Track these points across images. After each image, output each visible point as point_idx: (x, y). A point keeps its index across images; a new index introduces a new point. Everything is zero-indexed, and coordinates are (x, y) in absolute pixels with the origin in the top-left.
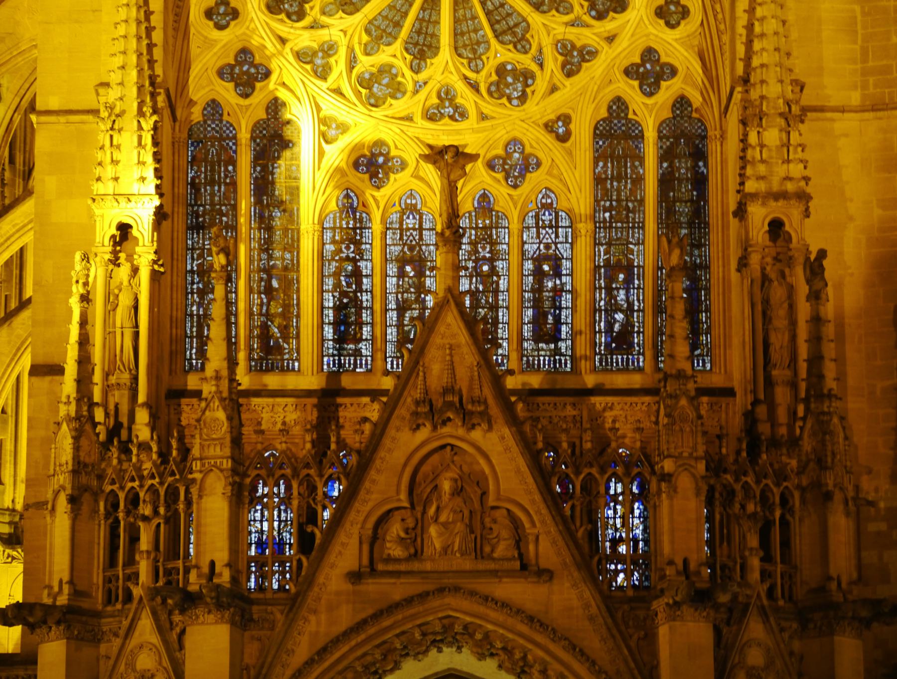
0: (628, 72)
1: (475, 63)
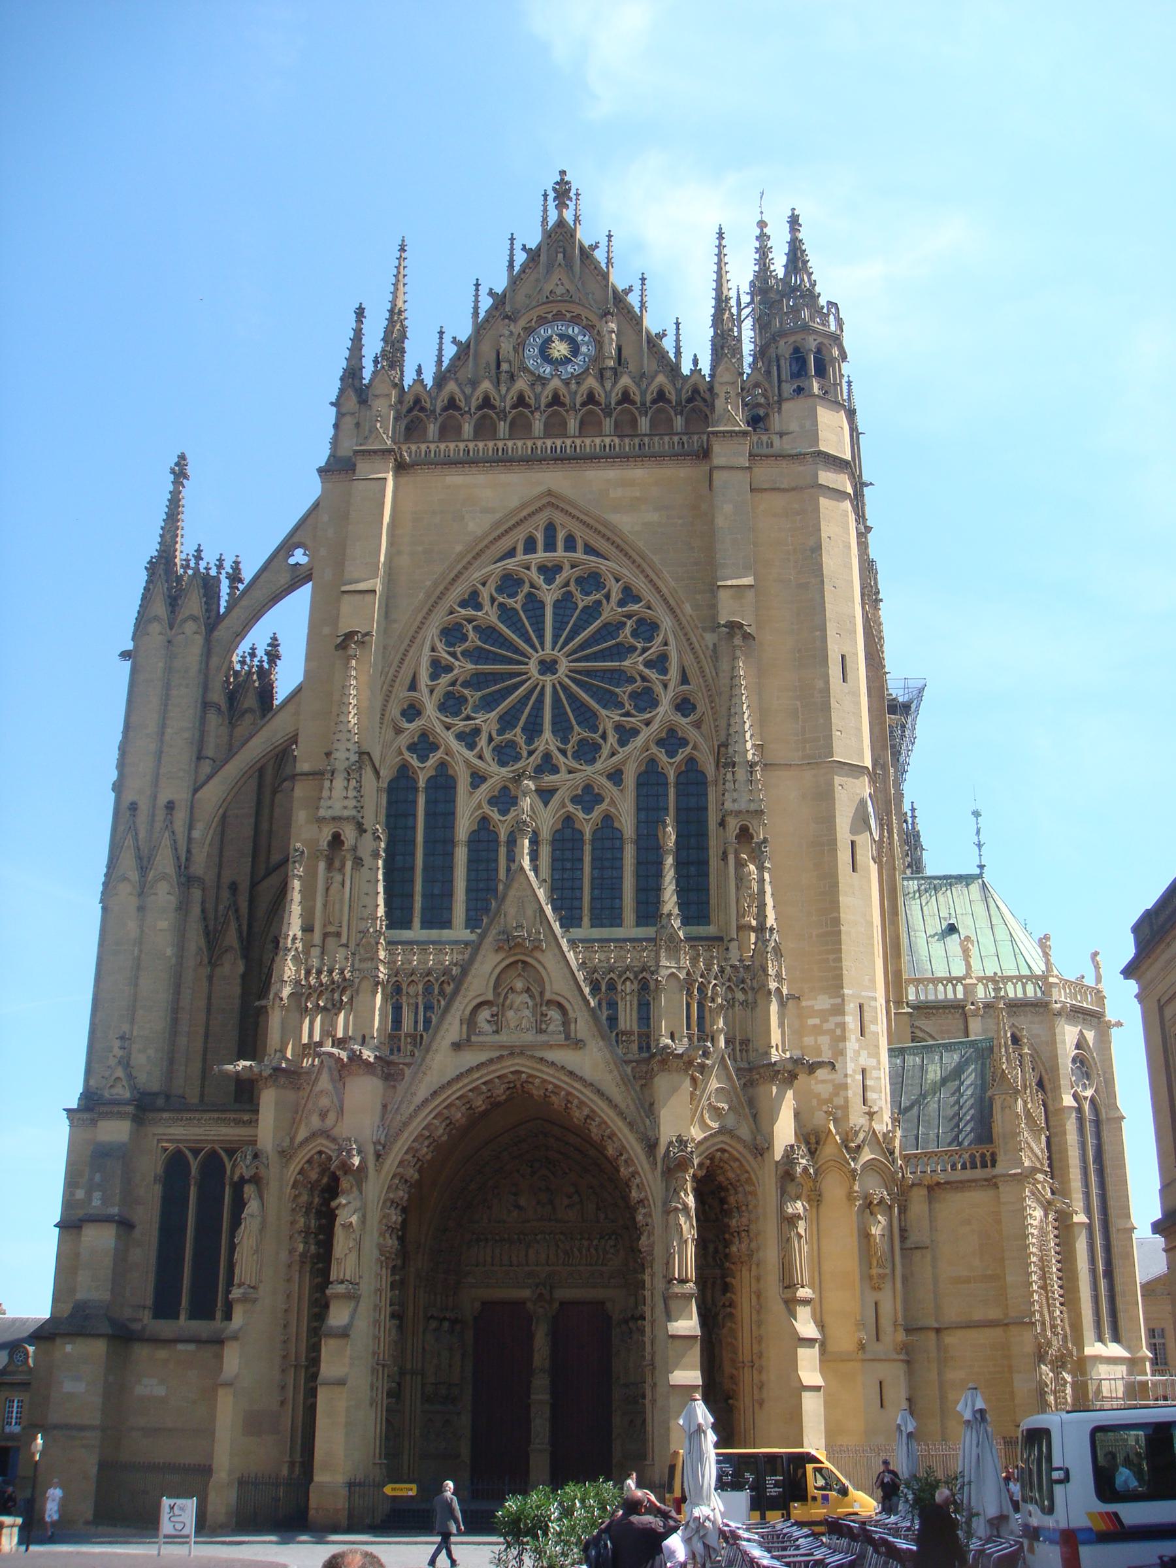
0: (660, 743)
1: (565, 741)
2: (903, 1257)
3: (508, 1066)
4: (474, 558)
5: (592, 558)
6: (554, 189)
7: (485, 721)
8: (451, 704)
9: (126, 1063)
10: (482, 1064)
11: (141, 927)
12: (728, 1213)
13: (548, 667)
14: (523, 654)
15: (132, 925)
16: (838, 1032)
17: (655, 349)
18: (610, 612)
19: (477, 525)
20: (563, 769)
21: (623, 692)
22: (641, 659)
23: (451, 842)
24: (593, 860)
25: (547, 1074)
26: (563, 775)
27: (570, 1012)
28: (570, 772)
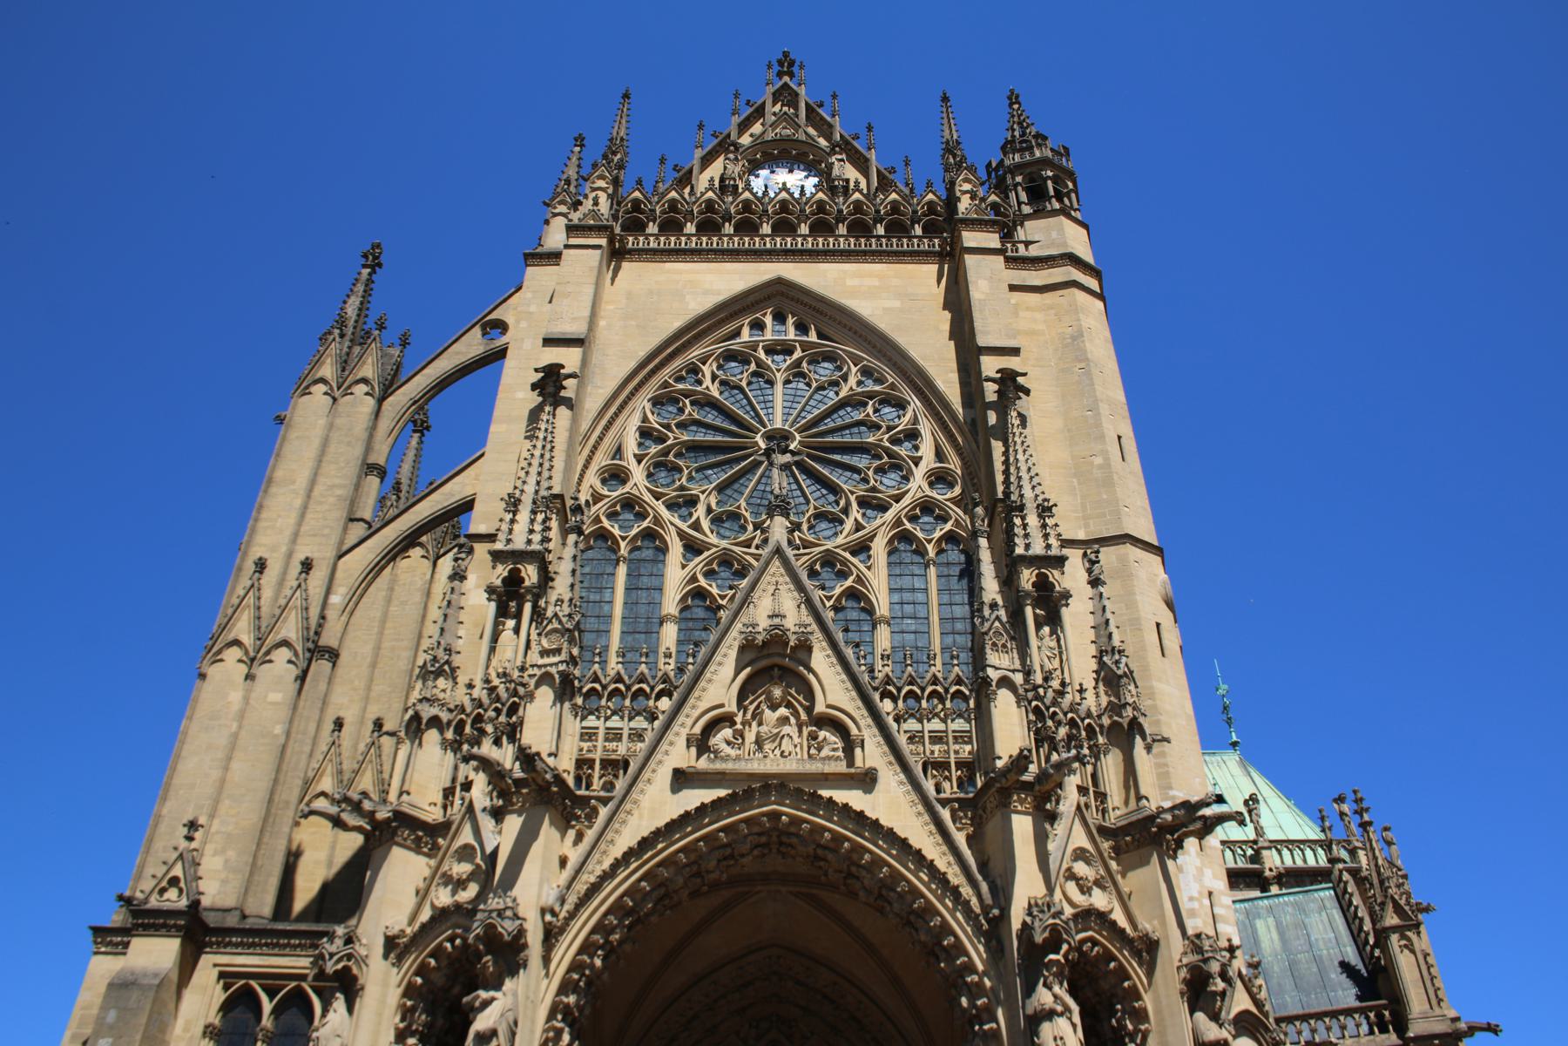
7: (703, 492)
11: (246, 700)
15: (236, 697)
17: (885, 181)
22: (887, 436)
27: (854, 731)
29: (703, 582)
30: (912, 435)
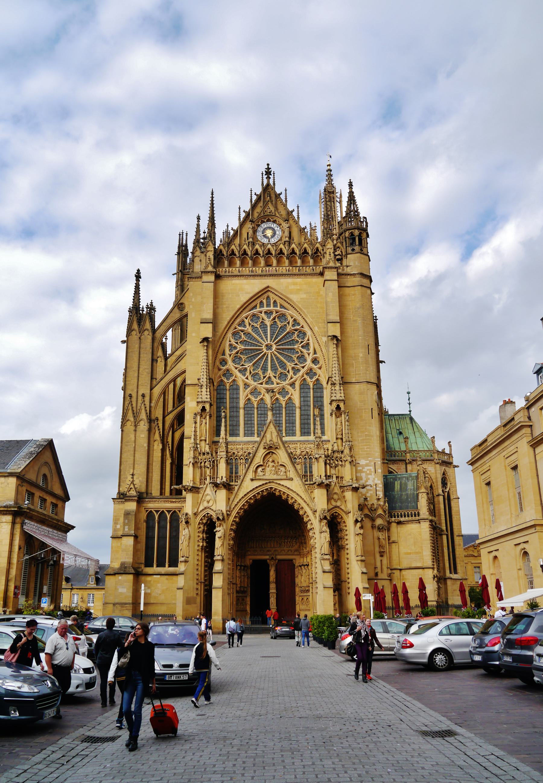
1: (275, 373)
2: (389, 545)
3: (268, 486)
4: (243, 310)
5: (283, 310)
6: (266, 171)
8: (236, 359)
9: (132, 482)
10: (260, 486)
11: (135, 437)
12: (338, 532)
13: (269, 347)
14: (261, 343)
15: (132, 436)
16: (368, 472)
18: (289, 328)
19: (244, 298)
20: (275, 383)
21: (294, 357)
22: (300, 345)
23: (238, 408)
24: (286, 414)
25: (280, 488)
26: (275, 385)
28: (278, 384)
29: (250, 396)
30: (308, 344)
